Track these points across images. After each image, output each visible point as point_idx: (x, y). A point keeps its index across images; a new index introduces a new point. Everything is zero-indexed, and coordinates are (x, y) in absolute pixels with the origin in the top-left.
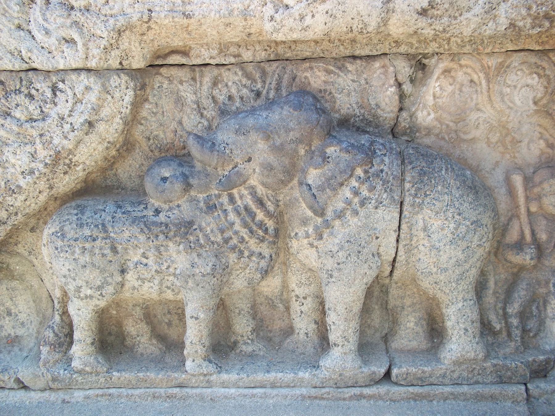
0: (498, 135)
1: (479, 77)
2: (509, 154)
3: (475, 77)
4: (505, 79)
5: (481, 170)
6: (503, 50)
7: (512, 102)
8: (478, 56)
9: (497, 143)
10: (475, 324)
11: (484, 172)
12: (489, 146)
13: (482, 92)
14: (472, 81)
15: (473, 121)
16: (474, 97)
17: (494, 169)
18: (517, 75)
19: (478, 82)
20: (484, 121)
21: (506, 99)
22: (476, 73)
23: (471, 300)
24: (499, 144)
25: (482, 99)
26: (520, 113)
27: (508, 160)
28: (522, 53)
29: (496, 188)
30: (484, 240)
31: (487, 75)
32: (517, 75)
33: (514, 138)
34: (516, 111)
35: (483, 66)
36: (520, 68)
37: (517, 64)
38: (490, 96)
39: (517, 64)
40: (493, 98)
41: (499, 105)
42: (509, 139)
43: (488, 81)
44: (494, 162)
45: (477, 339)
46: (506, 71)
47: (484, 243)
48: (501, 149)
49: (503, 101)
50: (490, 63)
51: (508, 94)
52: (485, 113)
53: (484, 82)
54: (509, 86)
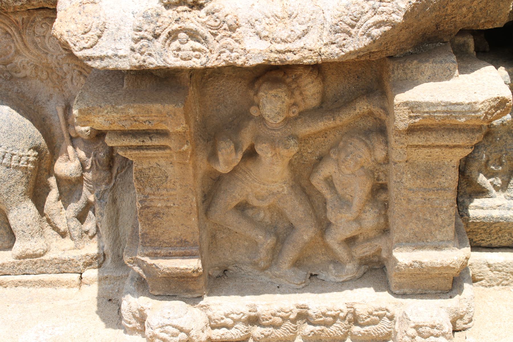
0: (45, 73)
1: (12, 30)
2: (58, 88)
3: (8, 29)
4: (34, 31)
5: (38, 102)
6: (23, 10)
7: (45, 49)
8: (5, 14)
9: (47, 79)
10: (30, 227)
11: (40, 103)
12: (43, 82)
13: (17, 41)
14: (7, 33)
15: (19, 63)
16: (12, 45)
17: (49, 101)
18: (42, 27)
19: (12, 34)
20: (28, 63)
21: (39, 45)
22: (8, 26)
23: (24, 208)
24: (49, 80)
25: (20, 46)
26: (55, 57)
27: (58, 93)
28: (42, 11)
29: (51, 115)
30: (22, 162)
31: (17, 29)
32: (42, 27)
33: (58, 76)
34: (52, 55)
35: (11, 21)
36: (45, 22)
37: (40, 20)
38: (25, 45)
39: (40, 20)
40: (29, 46)
41: (35, 51)
42: (55, 76)
43: (20, 34)
44: (49, 95)
45: (35, 239)
46: (32, 25)
47: (22, 164)
48: (51, 84)
49: (37, 48)
50: (17, 19)
51: (39, 43)
52: (26, 57)
53: (16, 34)
54: (38, 37)
